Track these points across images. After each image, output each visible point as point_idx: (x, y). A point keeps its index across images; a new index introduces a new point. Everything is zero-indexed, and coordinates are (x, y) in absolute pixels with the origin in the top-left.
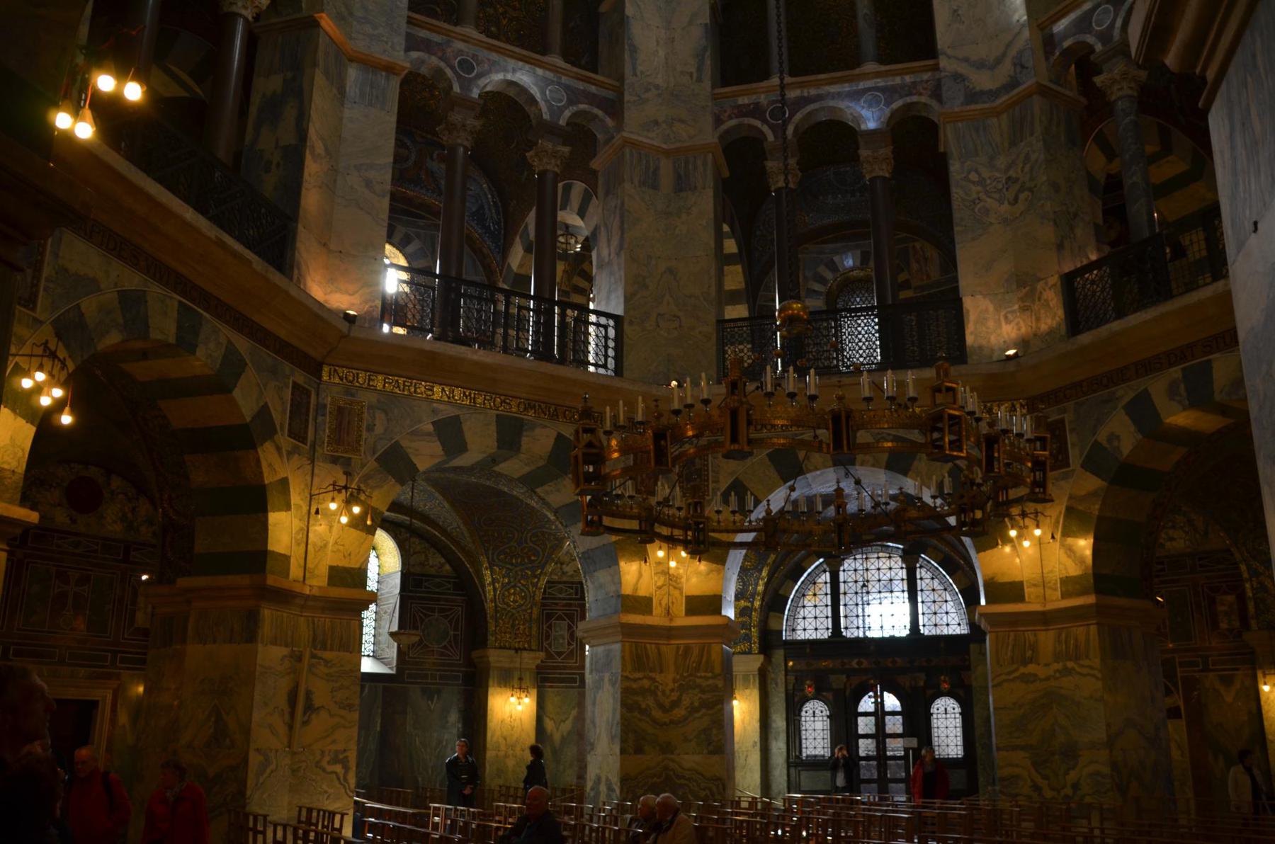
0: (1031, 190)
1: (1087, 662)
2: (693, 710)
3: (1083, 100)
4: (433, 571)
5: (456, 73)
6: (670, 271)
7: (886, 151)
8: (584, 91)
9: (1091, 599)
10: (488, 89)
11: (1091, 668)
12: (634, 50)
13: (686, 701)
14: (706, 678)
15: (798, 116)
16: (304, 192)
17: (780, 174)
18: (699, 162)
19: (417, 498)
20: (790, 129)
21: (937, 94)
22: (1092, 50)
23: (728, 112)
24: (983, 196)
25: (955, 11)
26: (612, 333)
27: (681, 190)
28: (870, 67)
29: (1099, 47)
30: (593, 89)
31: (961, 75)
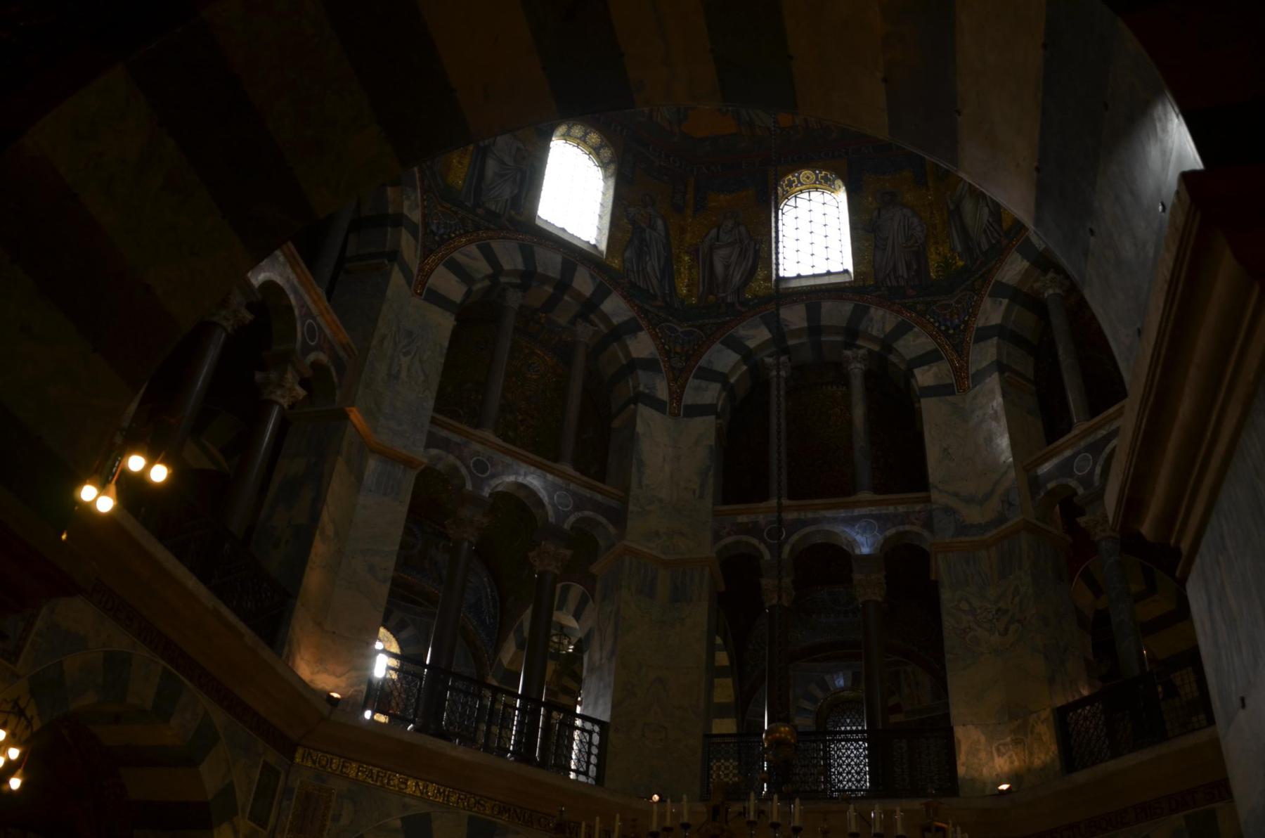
5: (470, 472)
10: (499, 489)
15: (795, 537)
16: (308, 569)
20: (786, 550)
21: (928, 524)
22: (1076, 494)
25: (945, 450)
26: (596, 739)
28: (865, 495)
29: (1081, 491)
30: (599, 497)
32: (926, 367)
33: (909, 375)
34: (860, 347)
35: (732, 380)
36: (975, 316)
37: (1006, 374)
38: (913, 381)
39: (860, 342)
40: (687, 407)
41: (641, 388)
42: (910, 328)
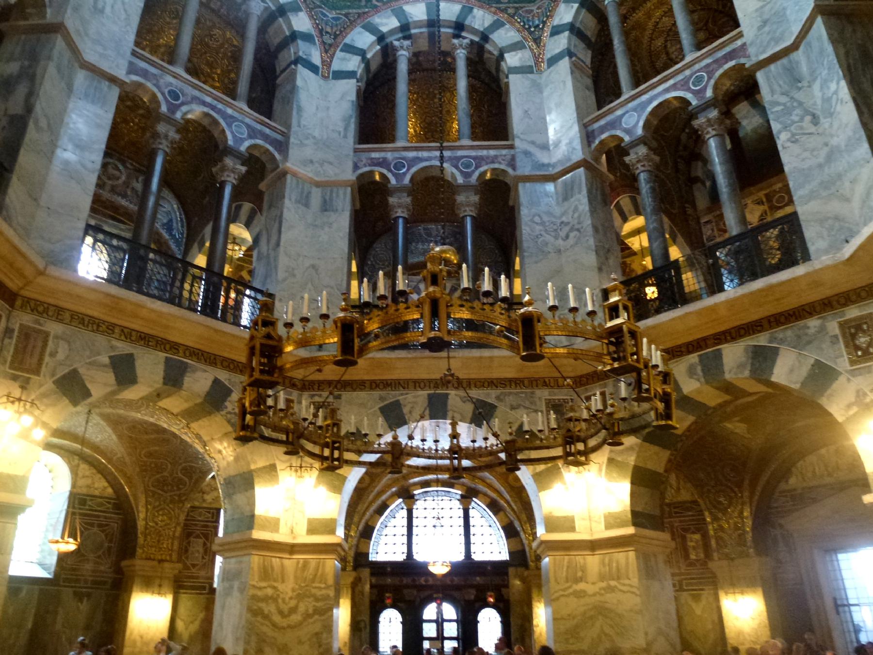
0: (578, 230)
1: (627, 582)
2: (307, 616)
3: (611, 177)
4: (97, 493)
6: (313, 266)
7: (475, 198)
8: (260, 131)
9: (630, 530)
11: (631, 586)
12: (300, 109)
13: (302, 608)
14: (320, 588)
17: (400, 206)
18: (341, 192)
19: (90, 430)
22: (622, 140)
23: (364, 161)
24: (543, 233)
27: (326, 210)
30: (267, 131)
31: (530, 153)
32: (513, 53)
33: (501, 57)
34: (464, 38)
35: (369, 56)
36: (552, 17)
37: (574, 59)
38: (503, 63)
39: (464, 34)
40: (334, 72)
41: (301, 54)
42: (503, 25)
